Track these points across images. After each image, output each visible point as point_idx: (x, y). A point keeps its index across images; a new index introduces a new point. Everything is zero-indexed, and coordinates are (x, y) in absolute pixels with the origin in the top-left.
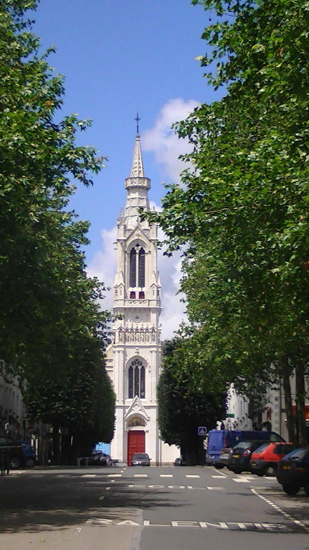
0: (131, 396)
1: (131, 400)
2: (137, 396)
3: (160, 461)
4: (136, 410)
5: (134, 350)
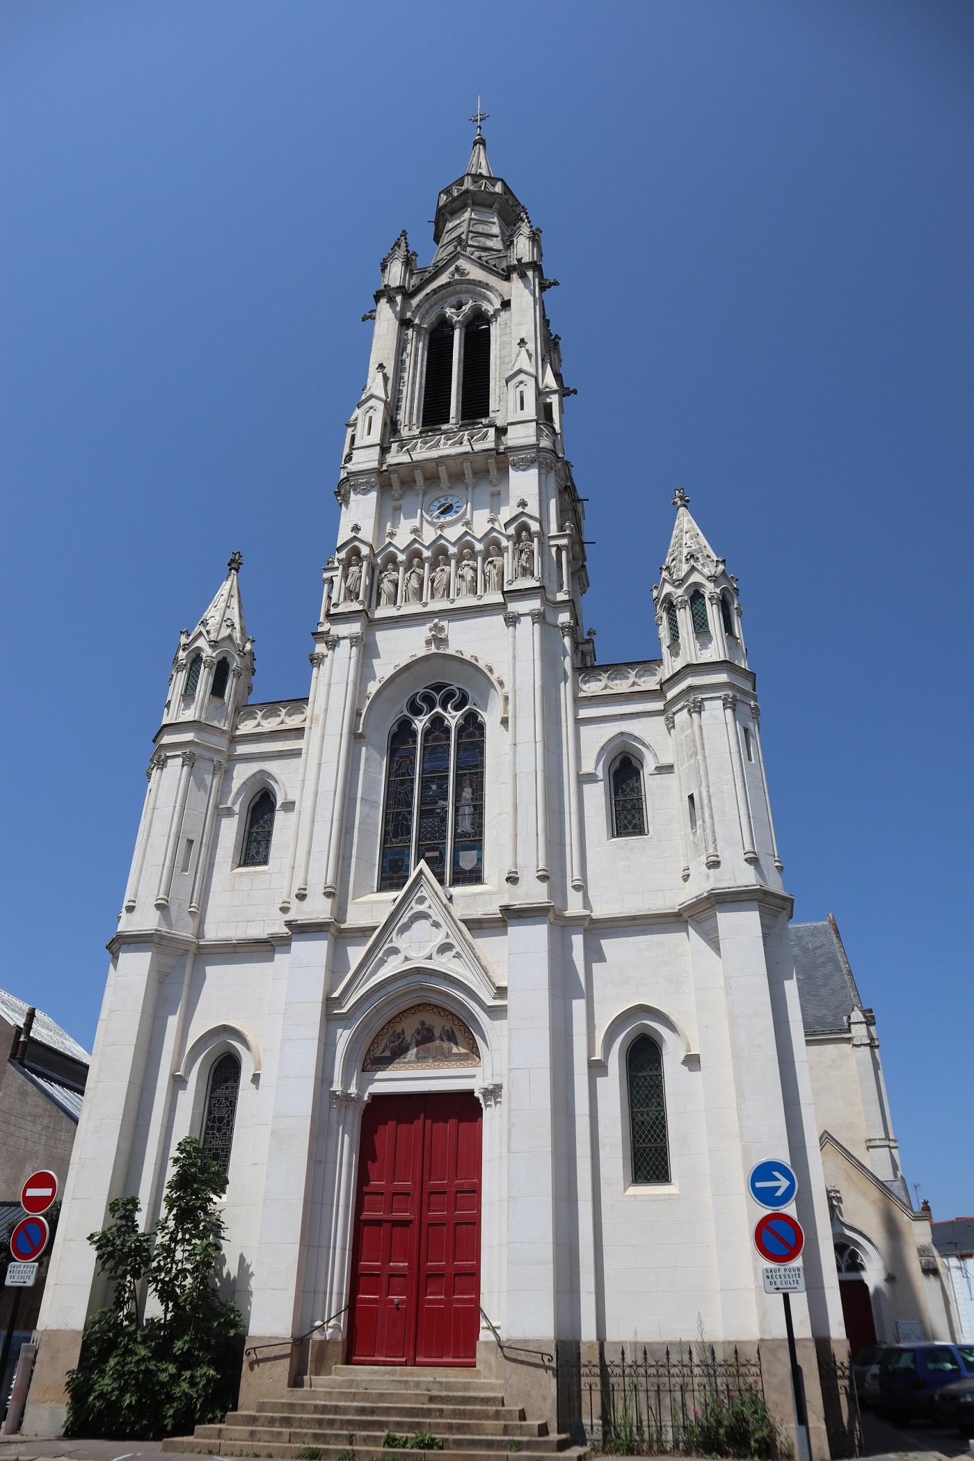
3: (588, 1333)
4: (417, 948)
5: (423, 632)
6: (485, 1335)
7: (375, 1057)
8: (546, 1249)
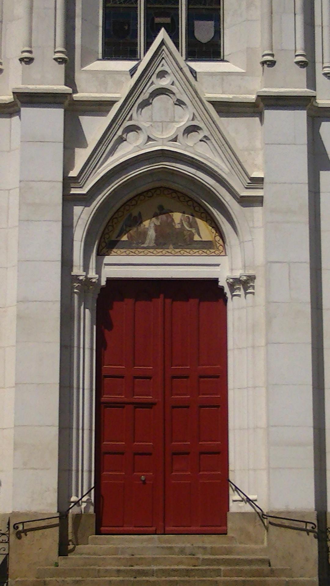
0: (119, 43)
1: (126, 65)
2: (162, 34)
4: (160, 129)
6: (236, 506)
7: (106, 237)
8: (309, 434)
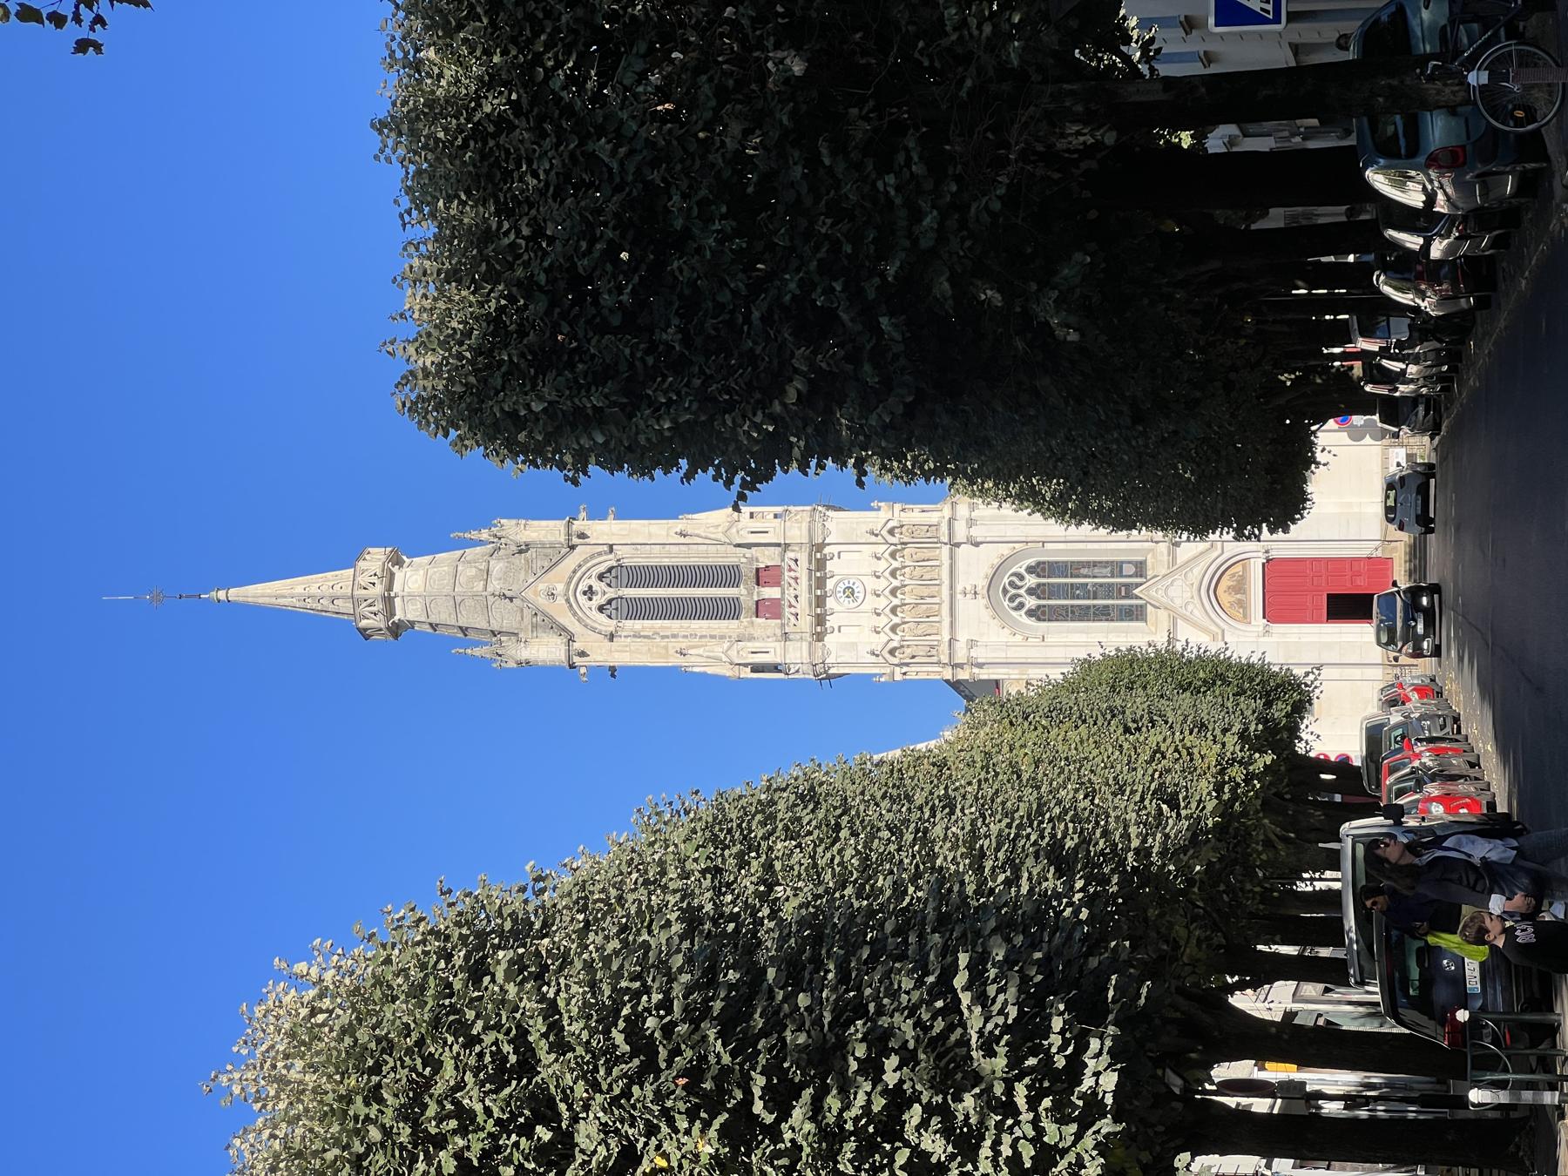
2: (1136, 592)
